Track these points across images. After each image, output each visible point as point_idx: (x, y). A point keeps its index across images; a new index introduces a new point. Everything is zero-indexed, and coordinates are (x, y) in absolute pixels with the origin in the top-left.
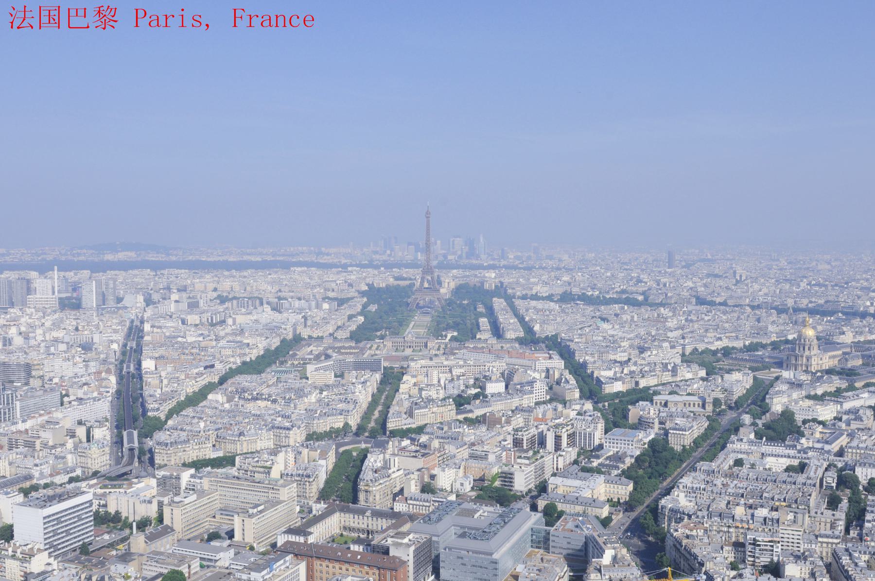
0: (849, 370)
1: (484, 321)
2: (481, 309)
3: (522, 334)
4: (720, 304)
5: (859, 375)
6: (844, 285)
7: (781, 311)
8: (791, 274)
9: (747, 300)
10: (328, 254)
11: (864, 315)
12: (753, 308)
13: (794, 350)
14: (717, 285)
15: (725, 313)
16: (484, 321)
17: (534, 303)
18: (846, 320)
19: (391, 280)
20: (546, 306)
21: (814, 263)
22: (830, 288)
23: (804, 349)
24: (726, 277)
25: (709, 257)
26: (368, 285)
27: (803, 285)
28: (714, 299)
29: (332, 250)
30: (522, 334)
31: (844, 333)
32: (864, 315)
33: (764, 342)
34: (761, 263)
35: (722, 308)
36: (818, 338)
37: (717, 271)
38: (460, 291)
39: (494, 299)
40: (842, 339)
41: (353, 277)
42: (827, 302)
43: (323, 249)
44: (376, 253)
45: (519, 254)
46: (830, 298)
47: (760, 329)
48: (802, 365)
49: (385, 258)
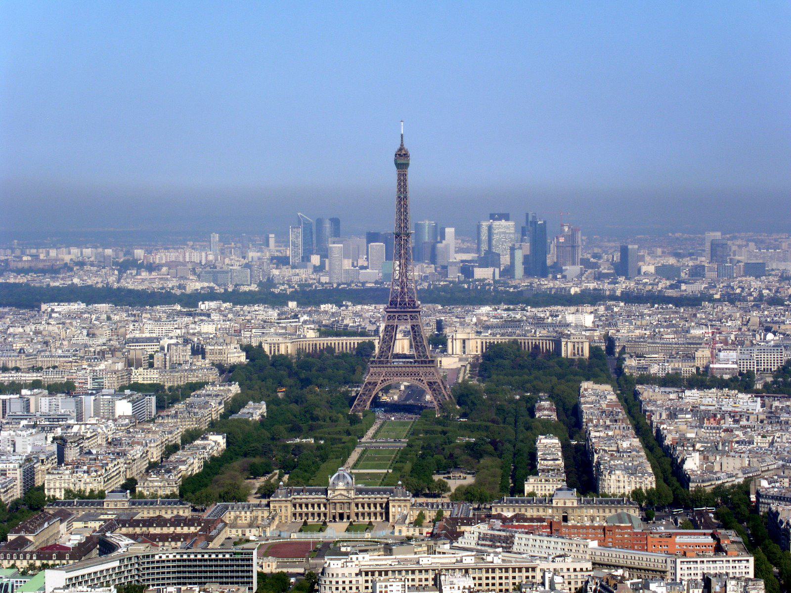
1: (549, 447)
2: (546, 410)
3: (649, 482)
10: (151, 268)
16: (549, 447)
17: (692, 396)
19: (311, 334)
20: (728, 406)
26: (247, 349)
29: (160, 257)
30: (649, 482)
38: (491, 360)
39: (585, 385)
41: (208, 328)
43: (139, 253)
44: (282, 261)
45: (672, 261)
49: (304, 274)
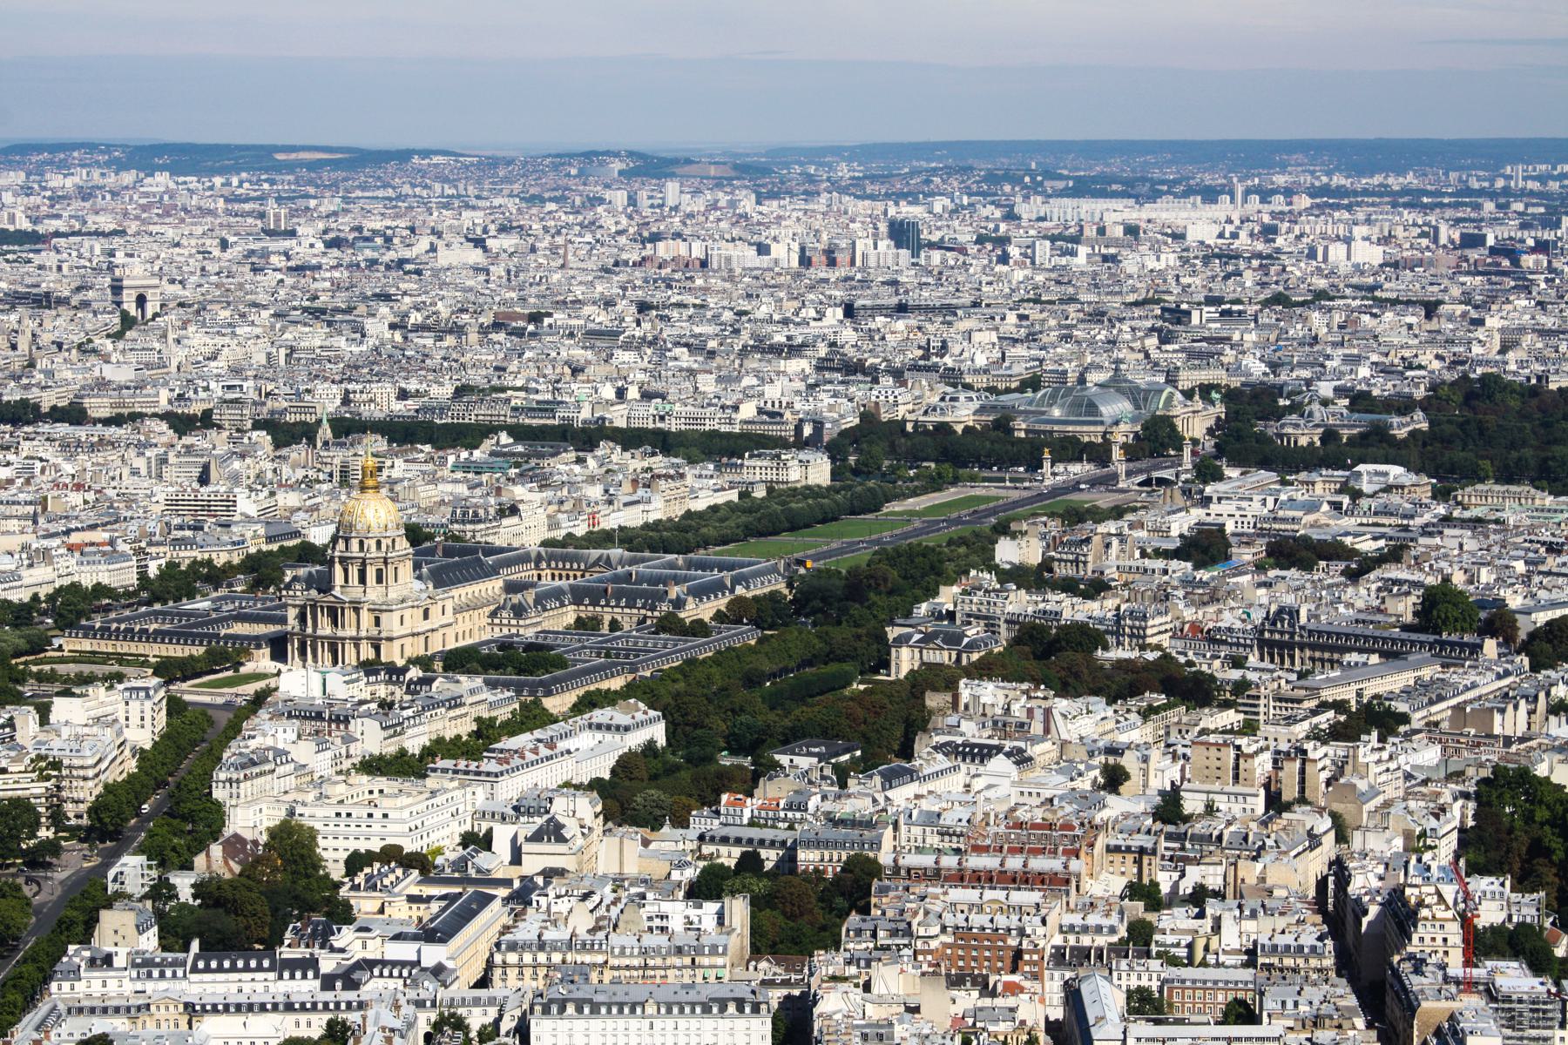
0: (530, 647)
4: (57, 415)
5: (561, 663)
6: (520, 326)
7: (286, 434)
8: (337, 286)
9: (164, 396)
11: (586, 438)
12: (182, 424)
13: (324, 584)
14: (46, 338)
15: (69, 448)
18: (528, 456)
21: (423, 244)
22: (473, 337)
23: (362, 580)
24: (85, 304)
25: (24, 225)
27: (378, 327)
28: (33, 395)
31: (514, 510)
32: (586, 438)
33: (220, 559)
34: (224, 245)
35: (63, 429)
36: (415, 534)
37: (49, 282)
40: (504, 534)
42: (461, 391)
46: (476, 377)
47: (207, 507)
48: (356, 641)
